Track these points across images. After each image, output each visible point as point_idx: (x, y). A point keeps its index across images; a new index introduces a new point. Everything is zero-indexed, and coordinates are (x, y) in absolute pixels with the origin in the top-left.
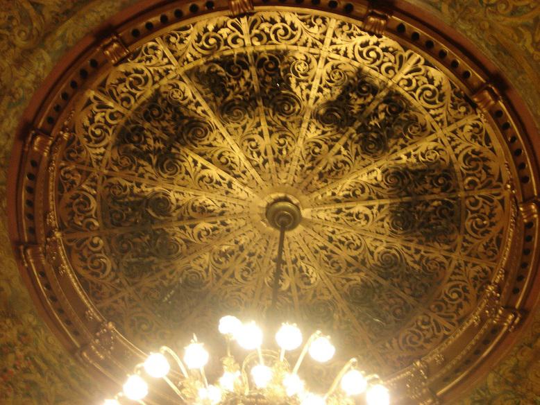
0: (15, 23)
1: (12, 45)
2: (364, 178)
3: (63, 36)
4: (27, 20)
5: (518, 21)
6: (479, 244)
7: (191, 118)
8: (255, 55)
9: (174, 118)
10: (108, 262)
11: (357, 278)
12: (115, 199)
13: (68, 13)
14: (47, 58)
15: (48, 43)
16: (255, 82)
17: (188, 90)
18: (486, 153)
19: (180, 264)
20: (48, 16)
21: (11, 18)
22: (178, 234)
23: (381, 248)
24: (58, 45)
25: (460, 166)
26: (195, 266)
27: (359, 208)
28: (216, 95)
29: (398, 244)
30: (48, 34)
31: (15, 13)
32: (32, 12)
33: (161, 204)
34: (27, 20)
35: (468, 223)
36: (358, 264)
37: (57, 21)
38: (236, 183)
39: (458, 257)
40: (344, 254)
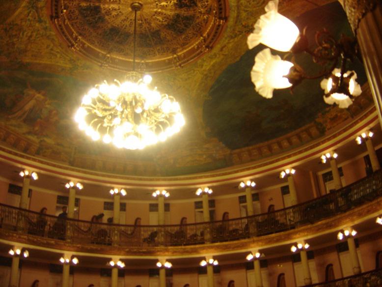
0: (248, 4)
3: (234, 11)
7: (182, 8)
8: (186, 30)
9: (186, 4)
13: (238, 16)
14: (233, 4)
15: (236, 8)
16: (179, 25)
17: (191, 13)
20: (241, 11)
21: (250, 4)
24: (233, 9)
28: (184, 17)
30: (238, 9)
31: (250, 6)
32: (246, 9)
34: (246, 7)
37: (239, 13)
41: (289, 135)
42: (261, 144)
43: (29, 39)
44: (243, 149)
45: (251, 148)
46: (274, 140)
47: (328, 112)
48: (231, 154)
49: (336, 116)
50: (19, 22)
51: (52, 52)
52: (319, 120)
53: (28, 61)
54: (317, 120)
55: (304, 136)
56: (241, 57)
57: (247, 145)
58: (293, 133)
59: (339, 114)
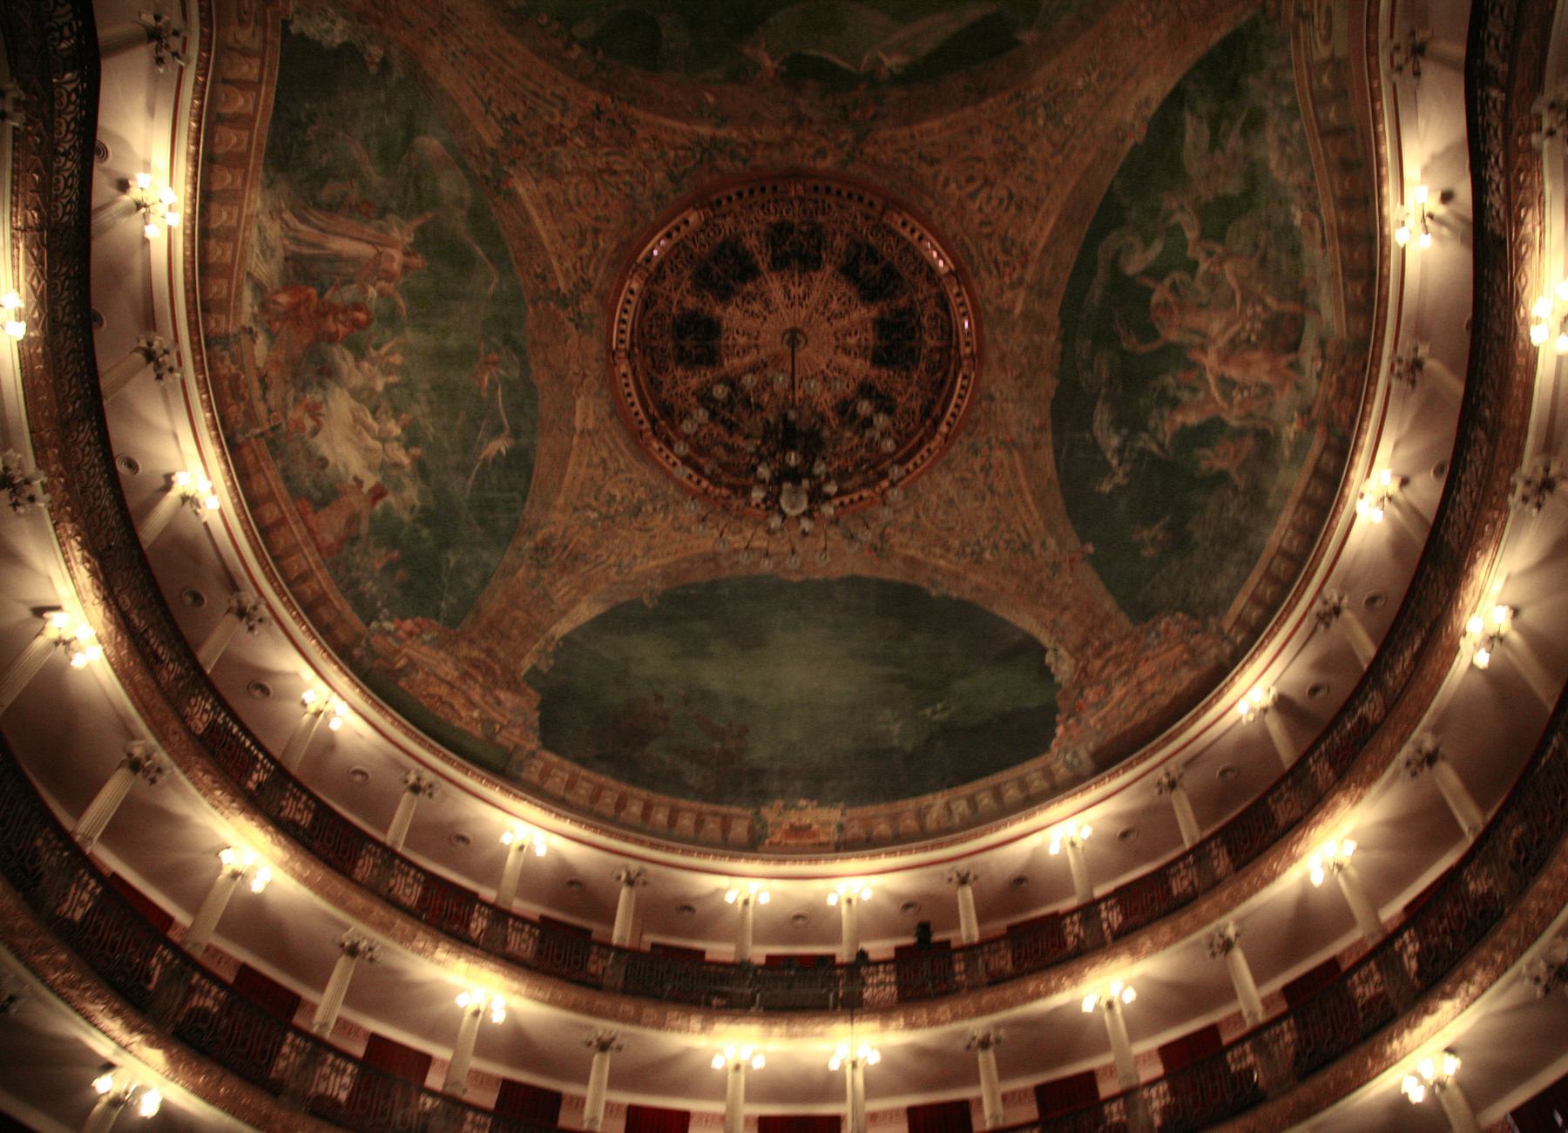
1: (939, 497)
2: (736, 361)
4: (926, 510)
5: (628, 475)
6: (661, 305)
10: (924, 321)
11: (750, 287)
12: (907, 369)
18: (654, 374)
19: (874, 313)
20: (912, 509)
22: (870, 337)
23: (730, 309)
25: (671, 364)
26: (864, 311)
27: (742, 340)
29: (718, 311)
33: (878, 360)
35: (668, 321)
36: (748, 298)
38: (823, 366)
39: (676, 297)
40: (757, 307)
41: (683, 803)
42: (612, 783)
43: (601, 171)
44: (567, 764)
45: (584, 772)
46: (644, 794)
47: (801, 809)
48: (533, 754)
49: (810, 826)
50: (640, 133)
51: (589, 236)
52: (769, 814)
53: (521, 190)
54: (765, 811)
55: (711, 826)
56: (807, 581)
57: (582, 762)
58: (696, 805)
59: (815, 827)
